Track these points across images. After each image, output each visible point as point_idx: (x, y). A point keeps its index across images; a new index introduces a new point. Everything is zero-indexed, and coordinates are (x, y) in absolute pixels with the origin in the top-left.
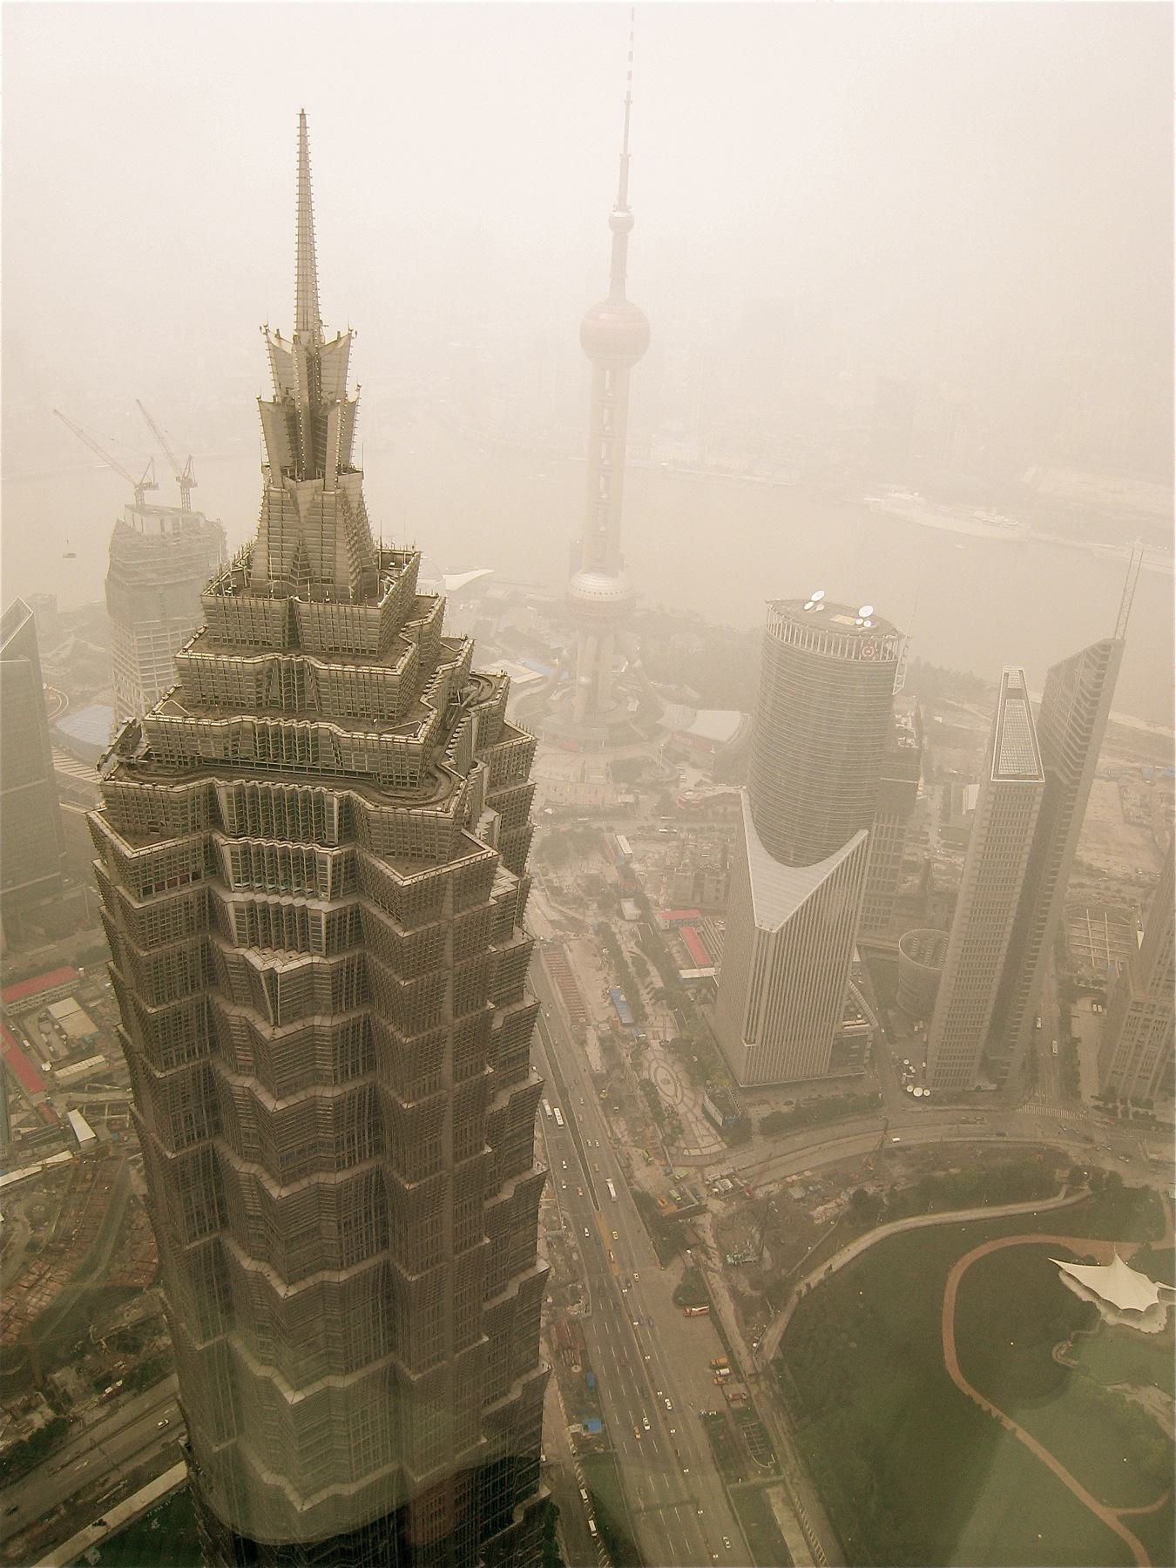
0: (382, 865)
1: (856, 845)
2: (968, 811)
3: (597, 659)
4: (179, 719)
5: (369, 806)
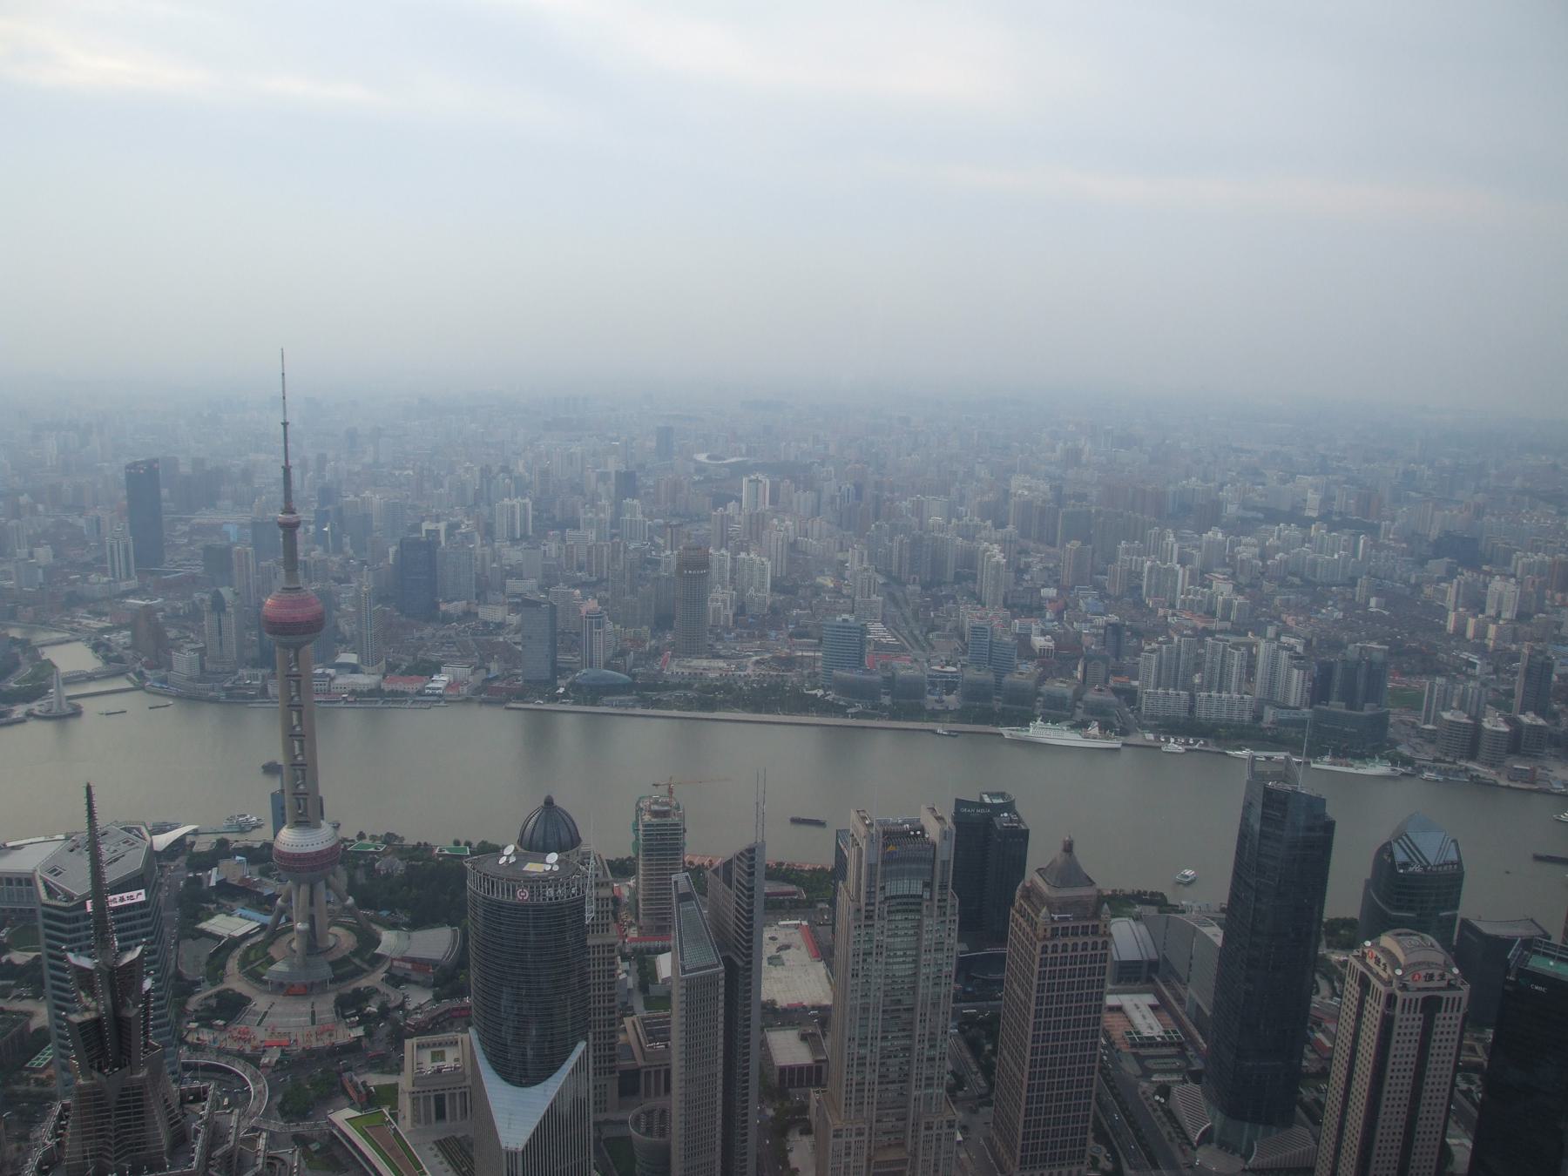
1: (574, 1062)
2: (666, 980)
3: (311, 903)
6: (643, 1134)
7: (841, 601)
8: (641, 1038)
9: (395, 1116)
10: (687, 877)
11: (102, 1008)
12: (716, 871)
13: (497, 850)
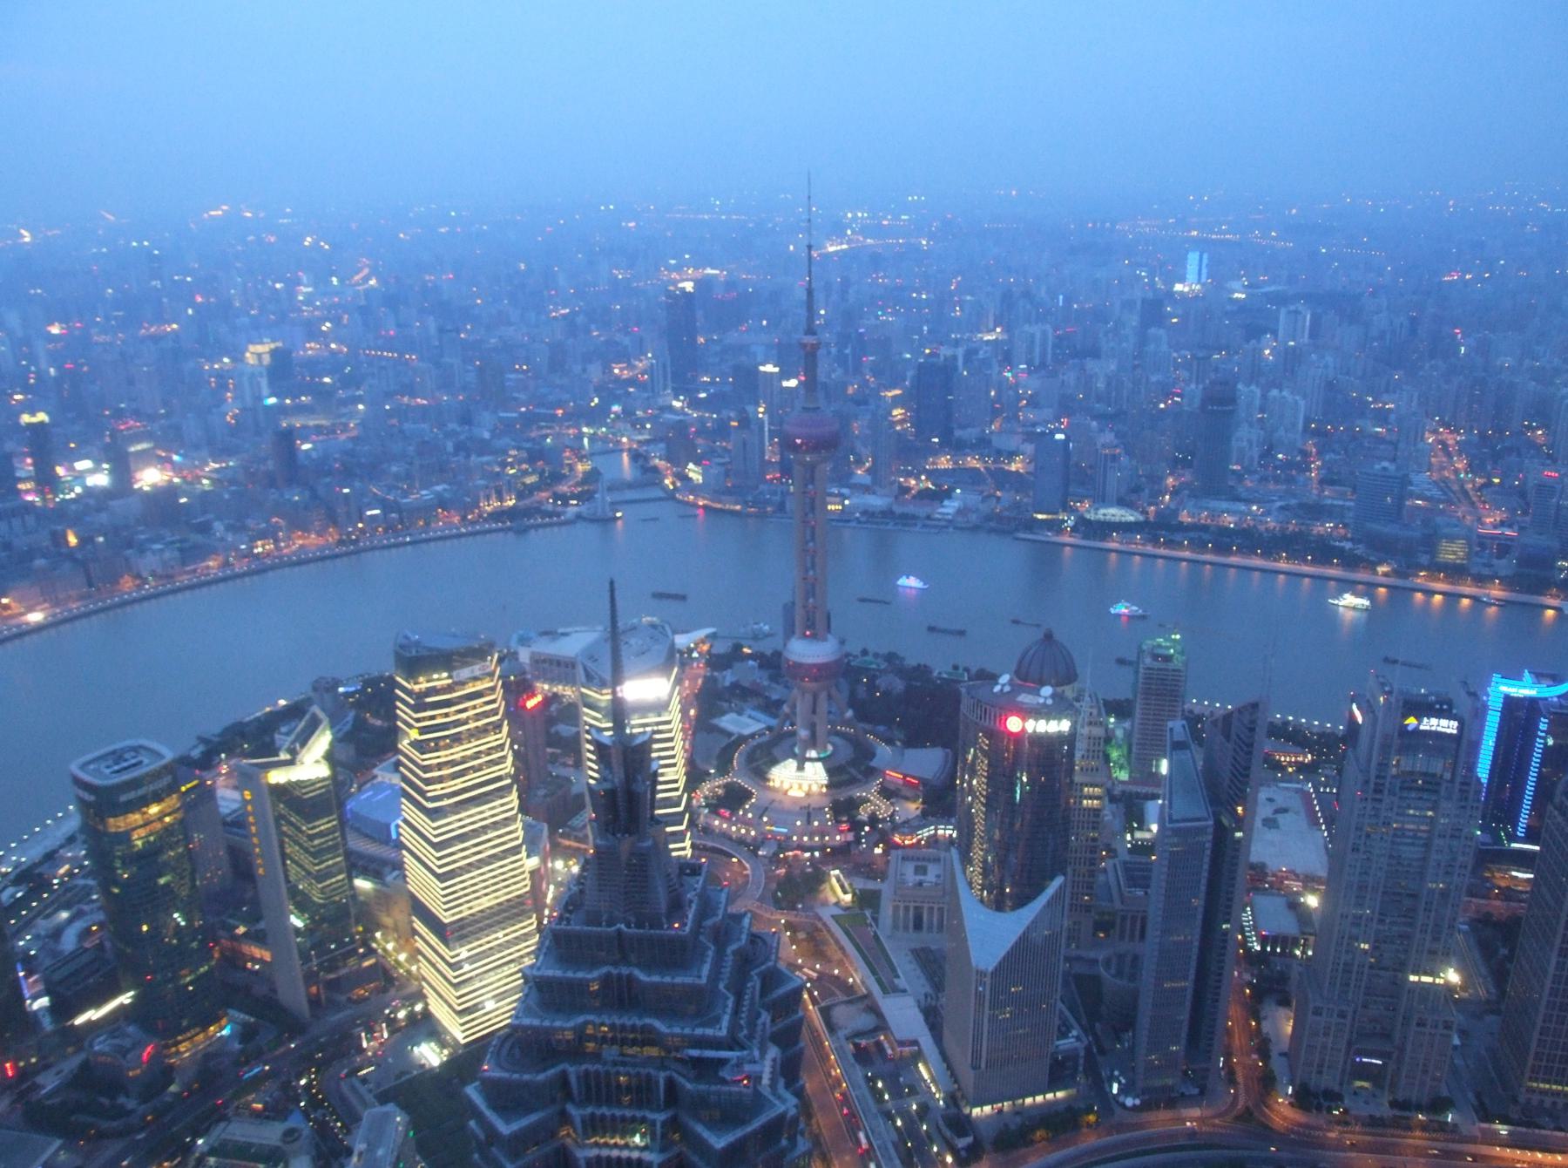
0: (700, 1129)
3: (814, 712)
4: (536, 1022)
5: (689, 1086)
6: (1113, 976)
7: (1382, 447)
8: (1121, 879)
9: (875, 920)
10: (1184, 726)
11: (616, 780)
12: (1214, 723)
13: (993, 678)
